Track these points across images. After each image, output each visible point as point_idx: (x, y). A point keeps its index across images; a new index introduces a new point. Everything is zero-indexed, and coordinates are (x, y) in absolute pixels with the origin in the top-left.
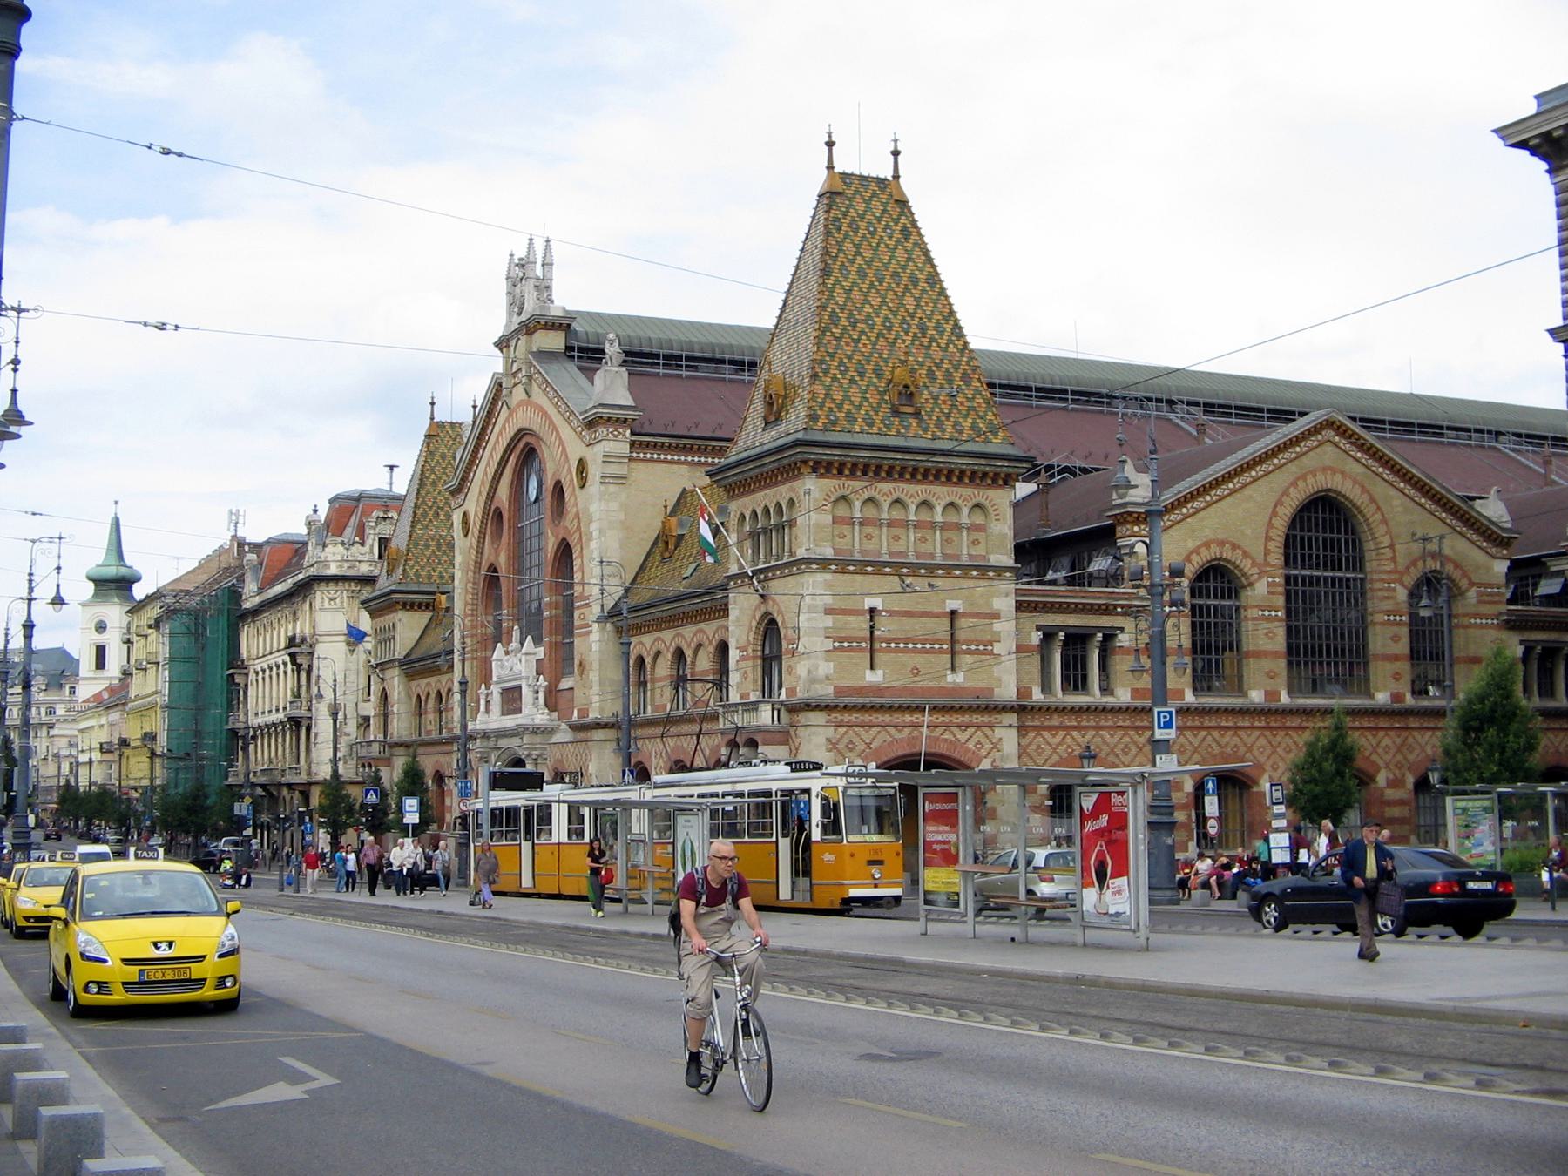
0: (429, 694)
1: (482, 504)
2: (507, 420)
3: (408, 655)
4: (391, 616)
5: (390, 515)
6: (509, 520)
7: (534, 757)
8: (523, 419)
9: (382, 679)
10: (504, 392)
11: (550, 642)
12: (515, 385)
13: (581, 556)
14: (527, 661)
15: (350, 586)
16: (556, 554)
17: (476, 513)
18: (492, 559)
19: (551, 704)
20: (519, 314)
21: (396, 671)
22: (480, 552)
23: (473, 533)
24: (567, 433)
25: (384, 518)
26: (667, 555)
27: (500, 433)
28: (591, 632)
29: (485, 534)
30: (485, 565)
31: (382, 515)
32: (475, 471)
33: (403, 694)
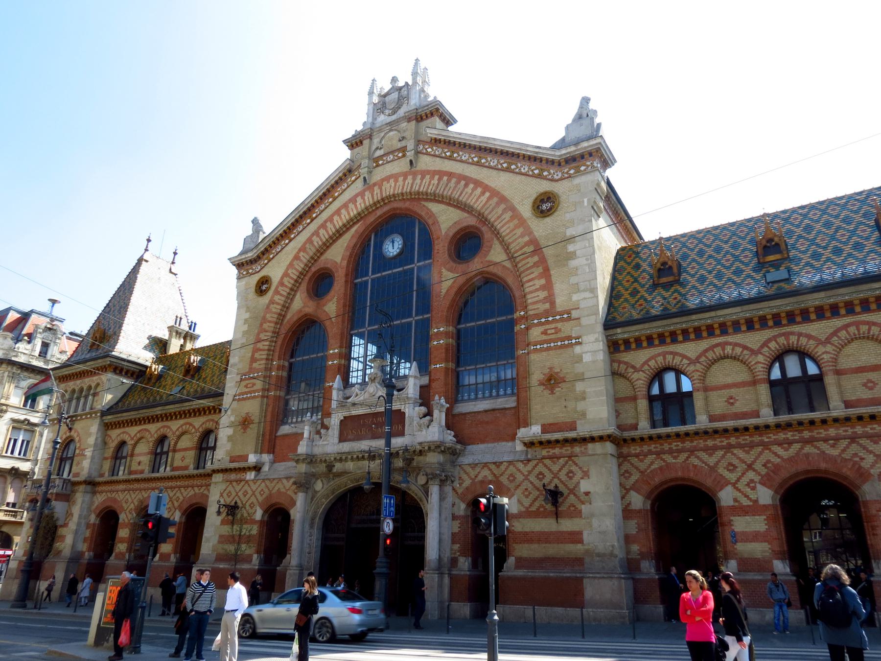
0: (142, 438)
1: (299, 266)
2: (361, 194)
3: (108, 410)
4: (95, 378)
5: (55, 328)
6: (347, 275)
7: (443, 477)
8: (389, 189)
9: (70, 429)
10: (364, 171)
11: (447, 369)
12: (378, 166)
13: (546, 273)
14: (415, 384)
15: (12, 369)
16: (460, 289)
17: (286, 274)
18: (310, 308)
19: (449, 426)
20: (394, 113)
21: (98, 421)
22: (286, 307)
23: (277, 292)
24: (500, 181)
25: (50, 329)
26: (664, 280)
27: (345, 206)
28: (580, 343)
29: (296, 291)
30: (292, 315)
31: (49, 326)
32: (287, 244)
33: (100, 440)
